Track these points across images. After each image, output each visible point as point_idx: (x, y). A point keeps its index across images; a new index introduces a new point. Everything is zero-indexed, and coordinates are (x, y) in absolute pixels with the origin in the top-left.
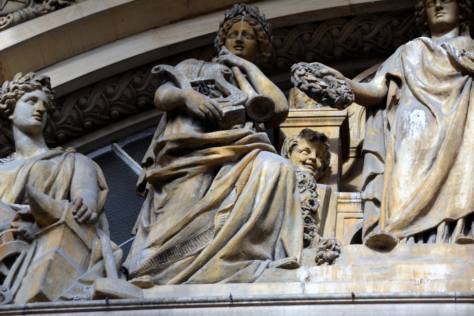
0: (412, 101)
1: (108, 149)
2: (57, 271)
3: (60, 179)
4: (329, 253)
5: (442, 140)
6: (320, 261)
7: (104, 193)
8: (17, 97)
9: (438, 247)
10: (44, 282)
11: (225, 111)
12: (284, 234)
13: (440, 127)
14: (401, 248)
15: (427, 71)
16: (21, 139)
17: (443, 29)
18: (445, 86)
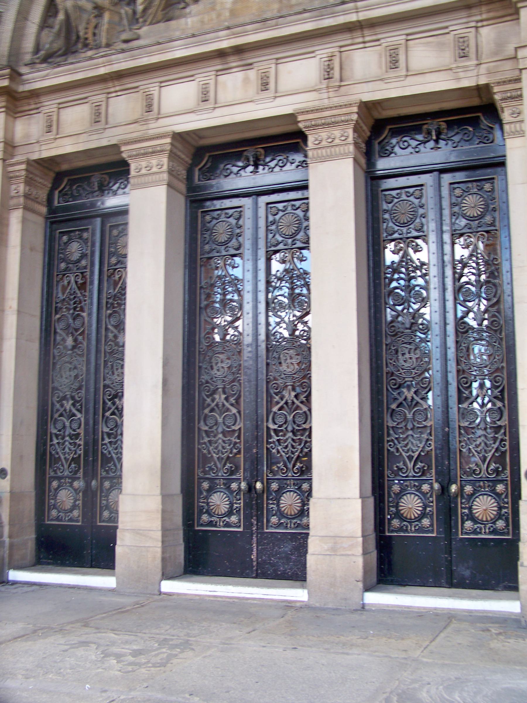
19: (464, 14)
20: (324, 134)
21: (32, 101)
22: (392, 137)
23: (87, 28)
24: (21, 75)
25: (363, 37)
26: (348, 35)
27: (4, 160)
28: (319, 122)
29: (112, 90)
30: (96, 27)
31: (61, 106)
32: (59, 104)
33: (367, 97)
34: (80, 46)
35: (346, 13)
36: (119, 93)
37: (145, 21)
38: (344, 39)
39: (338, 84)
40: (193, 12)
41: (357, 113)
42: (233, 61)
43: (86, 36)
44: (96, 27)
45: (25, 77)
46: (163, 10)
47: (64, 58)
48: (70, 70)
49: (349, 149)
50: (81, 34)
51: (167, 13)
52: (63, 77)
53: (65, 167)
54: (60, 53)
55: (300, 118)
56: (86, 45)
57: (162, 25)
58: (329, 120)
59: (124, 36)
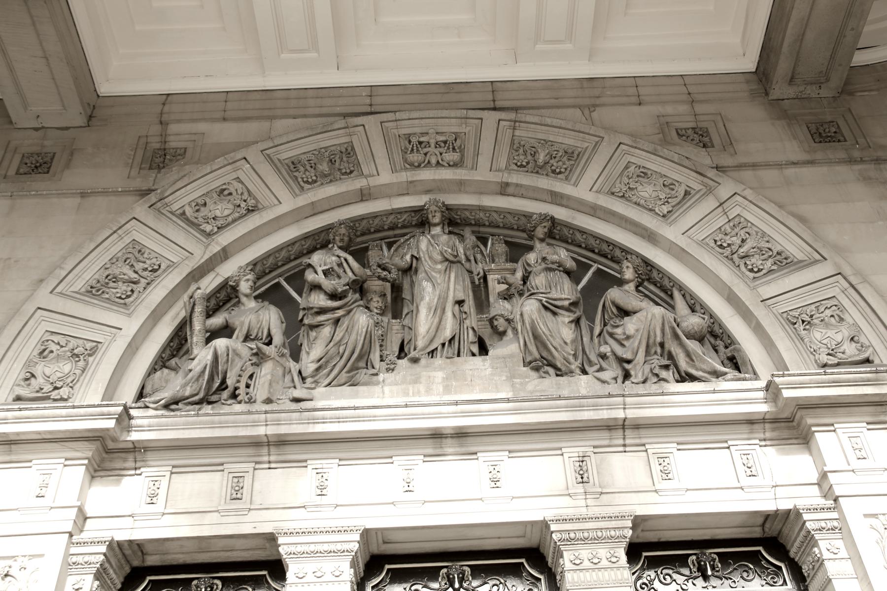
0: (423, 275)
1: (276, 281)
2: (274, 384)
3: (264, 323)
4: (392, 366)
5: (439, 299)
6: (388, 370)
7: (284, 325)
8: (240, 280)
9: (438, 361)
10: (269, 392)
11: (340, 290)
12: (371, 356)
13: (437, 293)
14: (423, 361)
15: (431, 258)
16: (244, 299)
17: (436, 225)
18: (439, 266)
19: (745, 428)
20: (585, 553)
21: (131, 457)
22: (649, 568)
23: (240, 376)
24: (130, 418)
25: (624, 439)
26: (606, 434)
27: (71, 535)
28: (580, 535)
29: (266, 459)
30: (251, 377)
31: (175, 470)
32: (174, 467)
33: (641, 511)
34: (225, 394)
35: (610, 407)
36: (273, 465)
37: (316, 382)
38: (602, 438)
39: (600, 490)
40: (388, 381)
41: (631, 528)
42: (450, 447)
43: (237, 385)
44: (251, 377)
45: (133, 422)
46: (348, 372)
47: (197, 407)
48: (213, 423)
49: (622, 574)
50: (230, 382)
51: (353, 377)
52: (198, 430)
53: (152, 560)
54: (196, 398)
55: (553, 527)
56: (234, 396)
57: (346, 388)
58: (592, 534)
59: (297, 394)
